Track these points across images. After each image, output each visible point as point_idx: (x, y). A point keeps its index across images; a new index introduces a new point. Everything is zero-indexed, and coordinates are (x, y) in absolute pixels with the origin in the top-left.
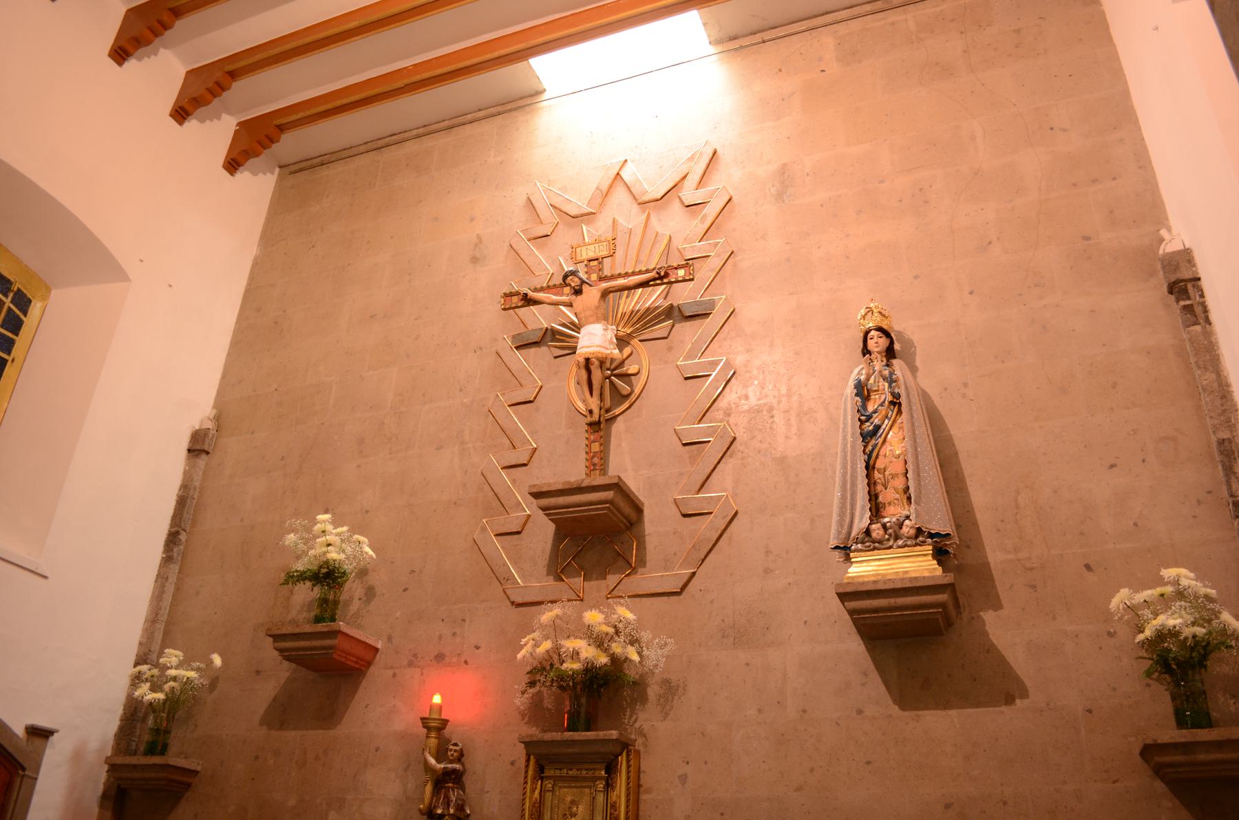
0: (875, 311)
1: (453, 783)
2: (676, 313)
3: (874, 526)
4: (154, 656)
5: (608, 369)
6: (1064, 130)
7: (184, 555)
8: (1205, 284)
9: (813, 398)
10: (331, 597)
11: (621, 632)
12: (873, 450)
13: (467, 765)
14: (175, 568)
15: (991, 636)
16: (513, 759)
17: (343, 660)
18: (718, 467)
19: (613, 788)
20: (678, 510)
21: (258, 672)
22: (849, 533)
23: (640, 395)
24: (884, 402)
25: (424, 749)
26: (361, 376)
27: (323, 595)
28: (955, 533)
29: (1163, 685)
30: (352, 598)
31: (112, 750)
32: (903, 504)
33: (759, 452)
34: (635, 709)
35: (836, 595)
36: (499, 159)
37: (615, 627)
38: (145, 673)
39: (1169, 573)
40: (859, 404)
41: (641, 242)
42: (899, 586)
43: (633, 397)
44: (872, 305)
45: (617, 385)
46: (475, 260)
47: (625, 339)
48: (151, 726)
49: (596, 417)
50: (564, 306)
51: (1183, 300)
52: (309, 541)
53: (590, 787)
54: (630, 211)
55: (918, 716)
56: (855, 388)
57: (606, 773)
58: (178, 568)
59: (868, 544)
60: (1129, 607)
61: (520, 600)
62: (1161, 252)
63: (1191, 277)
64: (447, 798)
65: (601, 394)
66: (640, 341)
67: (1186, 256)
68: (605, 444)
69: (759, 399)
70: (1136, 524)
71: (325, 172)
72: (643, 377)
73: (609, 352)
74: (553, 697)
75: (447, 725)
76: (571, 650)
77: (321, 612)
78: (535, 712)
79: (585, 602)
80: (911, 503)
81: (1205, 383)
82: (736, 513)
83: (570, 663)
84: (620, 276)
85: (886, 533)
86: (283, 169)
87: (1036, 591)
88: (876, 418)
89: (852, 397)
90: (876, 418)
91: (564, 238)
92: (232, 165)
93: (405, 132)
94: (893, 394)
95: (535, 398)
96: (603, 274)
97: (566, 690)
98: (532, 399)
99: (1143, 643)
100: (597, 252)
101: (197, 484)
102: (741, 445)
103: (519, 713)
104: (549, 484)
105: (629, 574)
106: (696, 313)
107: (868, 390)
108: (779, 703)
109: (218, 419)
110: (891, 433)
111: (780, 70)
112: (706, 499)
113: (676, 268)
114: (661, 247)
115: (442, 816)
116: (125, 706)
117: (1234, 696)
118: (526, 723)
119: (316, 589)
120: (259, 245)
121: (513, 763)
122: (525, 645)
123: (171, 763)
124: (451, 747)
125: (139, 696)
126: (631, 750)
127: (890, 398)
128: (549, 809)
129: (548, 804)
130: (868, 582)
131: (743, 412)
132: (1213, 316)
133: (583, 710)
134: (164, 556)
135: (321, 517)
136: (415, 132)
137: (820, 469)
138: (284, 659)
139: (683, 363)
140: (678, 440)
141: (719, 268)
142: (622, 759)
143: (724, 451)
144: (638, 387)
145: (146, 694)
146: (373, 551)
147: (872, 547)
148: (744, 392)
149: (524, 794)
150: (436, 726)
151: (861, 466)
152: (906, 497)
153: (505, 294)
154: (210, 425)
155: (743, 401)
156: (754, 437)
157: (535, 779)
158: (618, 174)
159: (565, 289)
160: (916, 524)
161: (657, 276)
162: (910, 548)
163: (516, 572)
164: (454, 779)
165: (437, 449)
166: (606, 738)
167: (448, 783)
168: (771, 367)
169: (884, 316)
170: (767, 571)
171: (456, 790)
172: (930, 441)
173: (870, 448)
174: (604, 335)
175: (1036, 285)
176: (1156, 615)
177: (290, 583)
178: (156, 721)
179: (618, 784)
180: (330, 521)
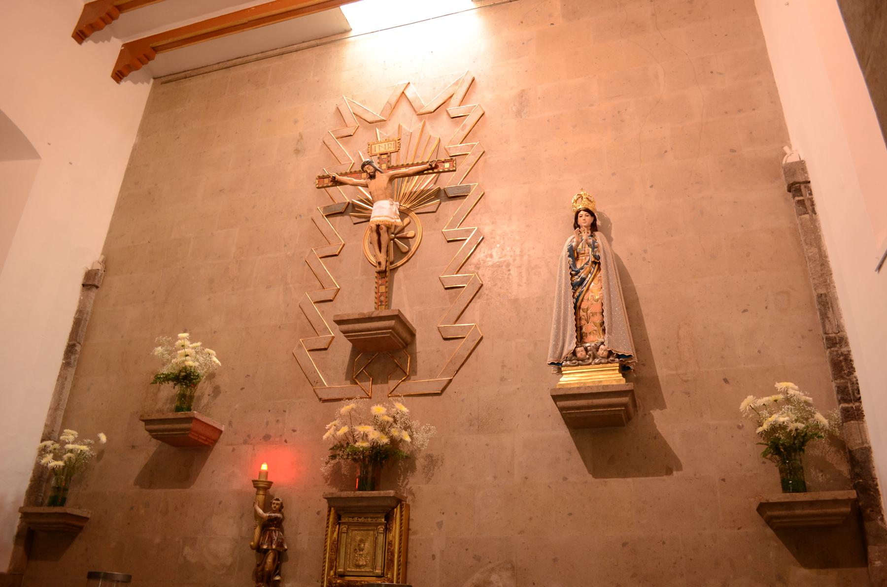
0: (584, 197)
1: (275, 527)
2: (442, 194)
3: (579, 349)
4: (56, 435)
5: (393, 233)
6: (720, 74)
7: (79, 362)
8: (813, 186)
9: (538, 258)
10: (188, 393)
11: (398, 421)
12: (580, 295)
13: (286, 515)
14: (72, 371)
15: (657, 428)
16: (319, 510)
17: (196, 439)
18: (469, 305)
19: (390, 531)
20: (440, 335)
21: (133, 447)
22: (561, 353)
23: (415, 252)
24: (588, 262)
25: (254, 502)
26: (212, 234)
27: (182, 392)
28: (635, 356)
29: (774, 462)
30: (203, 394)
31: (24, 502)
32: (599, 334)
33: (499, 295)
34: (407, 475)
35: (551, 397)
36: (317, 79)
37: (394, 417)
38: (49, 447)
39: (781, 385)
40: (571, 262)
41: (419, 143)
42: (595, 391)
43: (410, 254)
44: (582, 193)
45: (399, 245)
46: (297, 151)
47: (406, 212)
48: (54, 485)
49: (383, 268)
50: (361, 186)
51: (798, 196)
52: (172, 352)
53: (374, 530)
54: (411, 120)
55: (606, 482)
56: (568, 252)
57: (385, 521)
58: (74, 370)
59: (574, 361)
60: (753, 408)
61: (325, 397)
62: (784, 162)
63: (804, 180)
64: (271, 537)
65: (387, 251)
66: (416, 214)
67: (801, 166)
68: (389, 287)
69: (500, 258)
70: (759, 352)
71: (187, 83)
72: (417, 240)
73: (394, 221)
74: (348, 467)
75: (271, 485)
76: (362, 433)
77: (181, 404)
78: (335, 477)
79: (372, 399)
80: (605, 333)
81: (810, 254)
82: (482, 338)
83: (361, 442)
84: (403, 166)
85: (587, 354)
86: (157, 80)
87: (689, 396)
88: (583, 272)
89: (566, 258)
90: (583, 272)
91: (363, 137)
92: (119, 75)
93: (248, 56)
94: (595, 256)
95: (340, 252)
96: (390, 164)
97: (358, 462)
98: (337, 253)
99: (761, 434)
100: (387, 148)
101: (89, 309)
102: (486, 290)
103: (324, 477)
104: (349, 315)
105: (404, 380)
106: (457, 195)
107: (577, 253)
108: (509, 472)
109: (105, 262)
110: (592, 284)
111: (522, 22)
112: (461, 328)
113: (443, 162)
114: (433, 147)
115: (267, 550)
116: (34, 470)
117: (822, 471)
118: (329, 485)
119: (177, 387)
120: (137, 136)
121: (318, 513)
122: (329, 429)
123: (68, 512)
124: (274, 501)
125: (45, 463)
126: (403, 504)
127: (592, 259)
128: (344, 546)
129: (343, 541)
130: (574, 388)
131: (488, 266)
132: (818, 208)
133: (370, 475)
134: (64, 362)
135: (181, 335)
136: (255, 57)
137: (541, 308)
138: (153, 437)
139: (446, 230)
140: (442, 286)
141: (474, 163)
142: (397, 511)
143: (474, 293)
144: (414, 247)
145: (50, 461)
146: (219, 360)
147: (577, 364)
148: (489, 253)
149: (327, 535)
150: (263, 486)
151: (571, 306)
152: (601, 329)
153: (319, 177)
154: (99, 267)
155: (488, 259)
156: (496, 284)
157: (334, 524)
158: (403, 92)
159: (363, 174)
160: (608, 348)
161: (429, 167)
162: (604, 365)
163: (324, 378)
164: (276, 524)
165: (267, 288)
166: (386, 495)
167: (271, 527)
168: (510, 236)
169: (590, 201)
170: (502, 379)
171: (277, 532)
172: (620, 290)
173: (577, 294)
174: (390, 208)
175: (697, 183)
176: (771, 414)
177: (158, 382)
178: (57, 482)
179: (394, 528)
180: (188, 338)
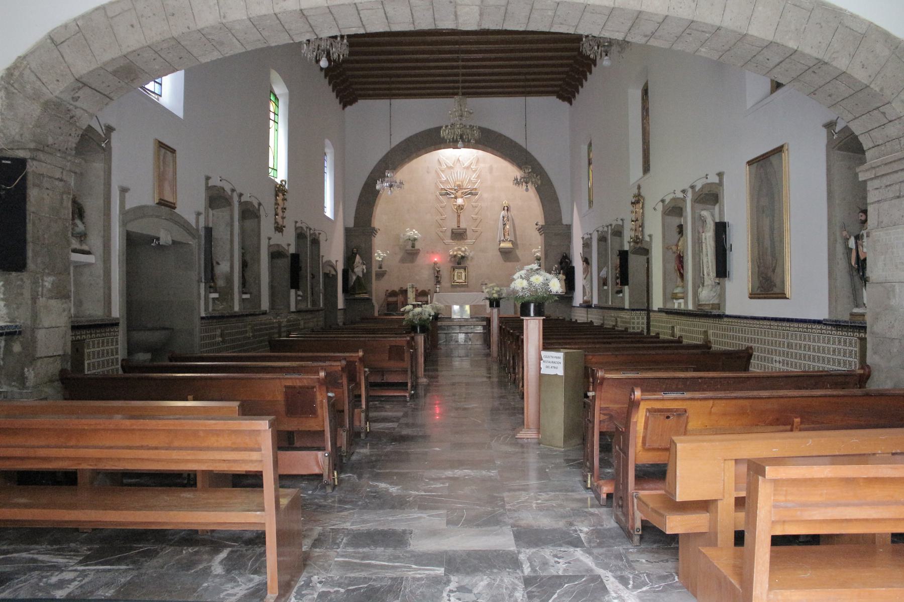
78: (451, 261)
150: (435, 263)
